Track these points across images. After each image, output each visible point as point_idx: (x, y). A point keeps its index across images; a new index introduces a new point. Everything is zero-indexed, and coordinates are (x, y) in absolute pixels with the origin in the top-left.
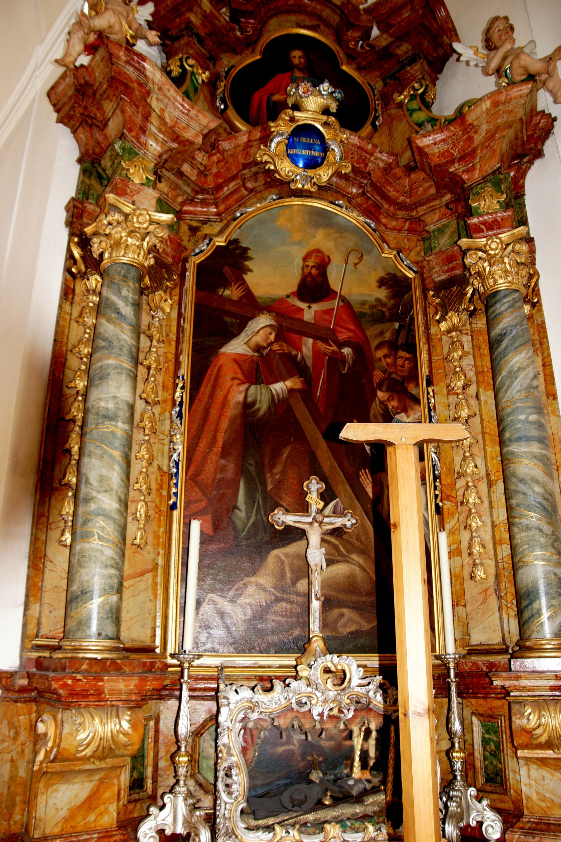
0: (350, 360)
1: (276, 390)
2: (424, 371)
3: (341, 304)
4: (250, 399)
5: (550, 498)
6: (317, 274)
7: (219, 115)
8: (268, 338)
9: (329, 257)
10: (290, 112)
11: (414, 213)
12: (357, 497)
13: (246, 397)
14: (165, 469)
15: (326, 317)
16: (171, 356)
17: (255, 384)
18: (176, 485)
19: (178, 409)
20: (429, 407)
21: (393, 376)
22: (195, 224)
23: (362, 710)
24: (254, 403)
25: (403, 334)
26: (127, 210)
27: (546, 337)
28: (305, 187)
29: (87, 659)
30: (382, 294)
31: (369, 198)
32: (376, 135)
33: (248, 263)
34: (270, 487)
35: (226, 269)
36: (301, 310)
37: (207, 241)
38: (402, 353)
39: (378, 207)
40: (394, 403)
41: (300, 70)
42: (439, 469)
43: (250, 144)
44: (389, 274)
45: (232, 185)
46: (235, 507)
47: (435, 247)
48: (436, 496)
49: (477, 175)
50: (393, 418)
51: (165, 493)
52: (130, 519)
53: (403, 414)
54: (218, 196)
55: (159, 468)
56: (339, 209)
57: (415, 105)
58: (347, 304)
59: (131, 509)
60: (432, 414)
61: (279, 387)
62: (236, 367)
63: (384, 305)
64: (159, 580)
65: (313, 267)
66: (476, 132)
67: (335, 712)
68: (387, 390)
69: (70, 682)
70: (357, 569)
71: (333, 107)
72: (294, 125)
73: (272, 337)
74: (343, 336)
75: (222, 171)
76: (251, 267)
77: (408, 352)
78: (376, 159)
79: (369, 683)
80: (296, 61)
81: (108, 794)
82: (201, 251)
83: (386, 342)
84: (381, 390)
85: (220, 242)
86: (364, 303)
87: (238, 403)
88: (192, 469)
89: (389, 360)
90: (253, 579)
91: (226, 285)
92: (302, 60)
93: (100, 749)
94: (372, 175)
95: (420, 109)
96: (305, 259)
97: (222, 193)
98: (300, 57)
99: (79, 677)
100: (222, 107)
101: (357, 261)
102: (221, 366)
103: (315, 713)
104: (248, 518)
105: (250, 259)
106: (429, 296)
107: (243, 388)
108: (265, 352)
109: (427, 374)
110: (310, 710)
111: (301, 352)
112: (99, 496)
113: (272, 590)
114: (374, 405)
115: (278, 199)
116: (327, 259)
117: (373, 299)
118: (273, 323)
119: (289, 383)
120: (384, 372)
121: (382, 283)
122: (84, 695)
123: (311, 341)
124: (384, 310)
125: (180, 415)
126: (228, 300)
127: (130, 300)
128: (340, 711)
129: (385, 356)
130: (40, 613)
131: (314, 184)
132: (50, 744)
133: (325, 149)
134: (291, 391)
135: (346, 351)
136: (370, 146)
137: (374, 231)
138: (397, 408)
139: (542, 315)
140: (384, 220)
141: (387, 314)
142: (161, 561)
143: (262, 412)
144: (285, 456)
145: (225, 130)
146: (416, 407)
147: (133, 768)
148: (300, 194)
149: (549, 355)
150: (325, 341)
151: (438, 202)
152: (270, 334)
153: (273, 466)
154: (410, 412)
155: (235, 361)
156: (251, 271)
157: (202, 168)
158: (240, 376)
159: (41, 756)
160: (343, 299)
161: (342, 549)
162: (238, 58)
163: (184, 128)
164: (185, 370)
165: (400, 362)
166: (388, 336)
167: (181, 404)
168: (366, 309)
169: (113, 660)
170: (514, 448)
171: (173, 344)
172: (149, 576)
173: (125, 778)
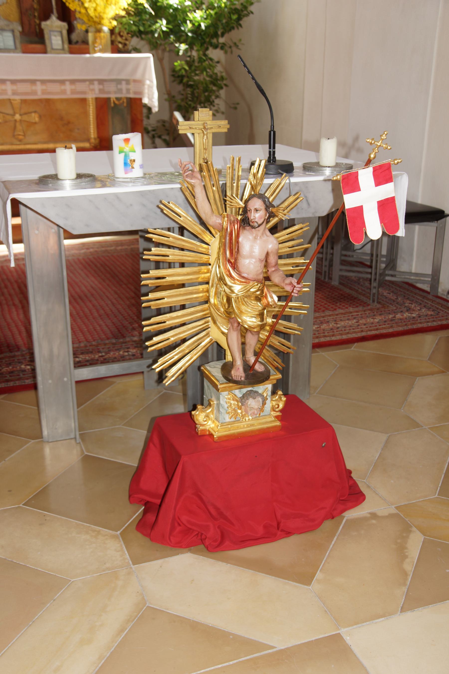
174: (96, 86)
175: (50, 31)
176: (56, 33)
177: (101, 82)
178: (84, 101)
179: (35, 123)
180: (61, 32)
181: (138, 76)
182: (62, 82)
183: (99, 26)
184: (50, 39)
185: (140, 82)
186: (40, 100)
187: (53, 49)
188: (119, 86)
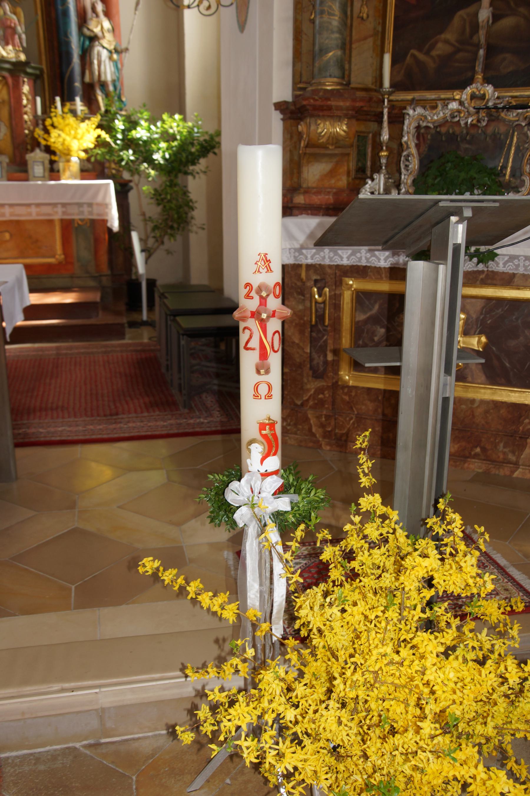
23: (493, 121)
29: (322, 89)
64: (379, 43)
67: (474, 122)
69: (312, 101)
90: (443, 36)
93: (331, 139)
99: (316, 98)
103: (462, 123)
110: (459, 120)
113: (457, 44)
122: (321, 108)
128: (479, 121)
132: (305, 136)
142: (380, 29)
147: (358, 161)
159: (302, 144)
169: (338, 90)
173: (352, 165)
174: (60, 209)
175: (34, 162)
176: (39, 164)
177: (64, 205)
178: (51, 222)
179: (6, 241)
180: (43, 163)
181: (99, 199)
182: (29, 205)
183: (68, 157)
184: (33, 169)
185: (106, 206)
186: (11, 222)
187: (34, 177)
188: (81, 209)
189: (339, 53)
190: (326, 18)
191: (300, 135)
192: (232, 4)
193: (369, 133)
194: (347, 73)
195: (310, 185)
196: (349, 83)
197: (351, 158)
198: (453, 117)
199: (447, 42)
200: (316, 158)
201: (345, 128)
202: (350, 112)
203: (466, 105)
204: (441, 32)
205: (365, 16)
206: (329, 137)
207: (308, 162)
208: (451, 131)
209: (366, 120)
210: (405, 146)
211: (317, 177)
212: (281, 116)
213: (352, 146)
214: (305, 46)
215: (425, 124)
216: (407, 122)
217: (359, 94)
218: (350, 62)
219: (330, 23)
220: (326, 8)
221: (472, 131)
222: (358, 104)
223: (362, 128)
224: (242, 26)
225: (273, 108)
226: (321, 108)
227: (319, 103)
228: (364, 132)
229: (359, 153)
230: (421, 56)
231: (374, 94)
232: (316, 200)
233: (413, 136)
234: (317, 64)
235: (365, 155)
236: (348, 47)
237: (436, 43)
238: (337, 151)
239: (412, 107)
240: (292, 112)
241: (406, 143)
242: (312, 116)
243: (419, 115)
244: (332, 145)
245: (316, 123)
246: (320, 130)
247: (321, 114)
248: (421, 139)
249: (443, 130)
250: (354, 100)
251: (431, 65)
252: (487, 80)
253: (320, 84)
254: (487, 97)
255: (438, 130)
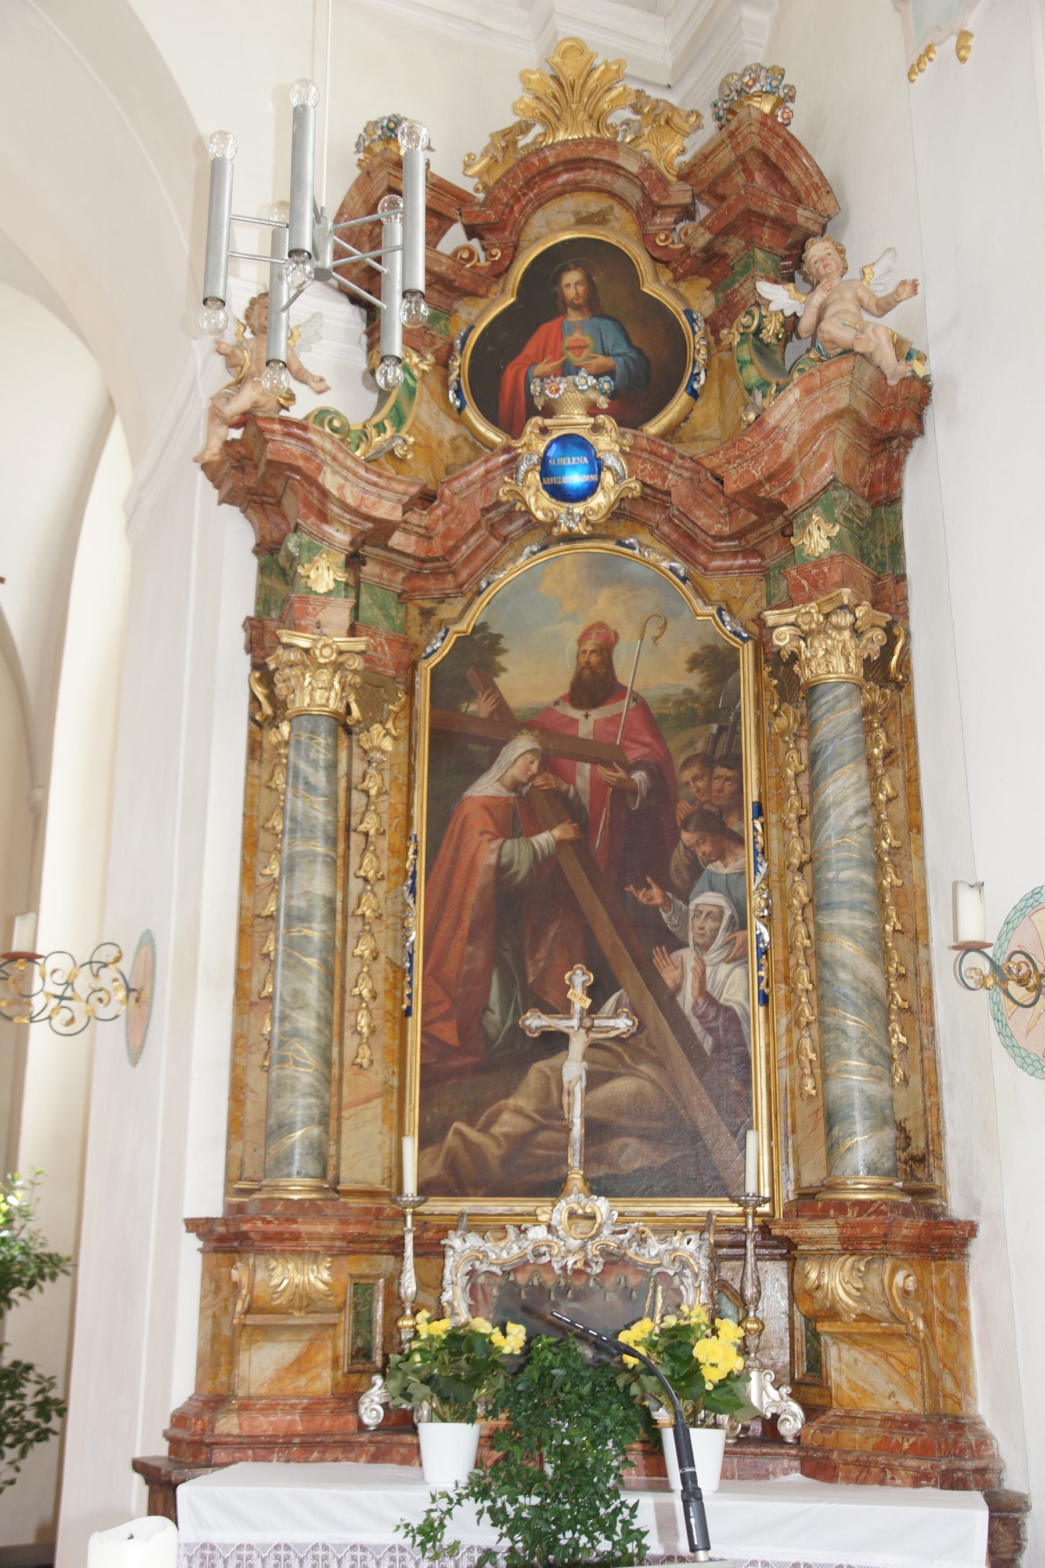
0: (643, 789)
1: (539, 844)
2: (752, 794)
3: (633, 705)
4: (504, 860)
5: (862, 987)
6: (599, 663)
7: (456, 415)
8: (528, 769)
9: (616, 634)
10: (538, 420)
11: (743, 543)
12: (649, 988)
13: (499, 857)
14: (399, 963)
15: (611, 729)
16: (401, 808)
17: (512, 837)
18: (410, 983)
19: (410, 882)
20: (755, 849)
21: (707, 806)
22: (427, 604)
23: (614, 1263)
24: (510, 864)
25: (724, 739)
26: (305, 643)
27: (914, 736)
28: (576, 529)
29: (281, 1199)
30: (694, 681)
31: (677, 526)
32: (700, 402)
33: (501, 659)
34: (531, 980)
35: (471, 674)
36: (574, 722)
37: (442, 634)
38: (721, 771)
39: (692, 540)
40: (706, 848)
41: (577, 308)
42: (767, 938)
43: (490, 476)
44: (707, 647)
45: (473, 540)
46: (487, 1008)
47: (775, 595)
48: (760, 979)
49: (802, 497)
50: (703, 870)
51: (398, 994)
52: (347, 1033)
53: (718, 863)
54: (453, 561)
55: (391, 962)
56: (630, 551)
57: (746, 353)
58: (641, 705)
59: (349, 1020)
60: (759, 859)
61: (544, 839)
62: (486, 816)
63: (696, 699)
64: (394, 1106)
65: (593, 652)
66: (785, 438)
67: (579, 1265)
68: (698, 828)
69: (259, 1224)
70: (647, 1084)
71: (603, 402)
72: (548, 440)
73: (534, 768)
74: (634, 754)
75: (453, 526)
76: (504, 665)
77: (728, 767)
78: (677, 466)
79: (625, 1231)
80: (570, 293)
81: (320, 1358)
82: (434, 651)
83: (696, 756)
84: (686, 829)
85: (465, 626)
86: (665, 700)
87: (489, 867)
88: (431, 961)
89: (700, 784)
90: (511, 1102)
91: (471, 696)
92: (581, 289)
93: (297, 1297)
94: (673, 494)
95: (751, 362)
96: (581, 641)
97: (458, 556)
98: (577, 283)
99: (269, 1217)
100: (458, 403)
101: (657, 633)
102: (466, 817)
103: (556, 1267)
104: (503, 1023)
105: (504, 651)
106: (765, 674)
107: (495, 845)
108: (525, 790)
109: (756, 799)
111: (574, 784)
112: (294, 1014)
114: (675, 853)
115: (539, 551)
116: (613, 636)
117: (680, 691)
118: (536, 746)
119: (557, 833)
120: (692, 803)
121: (694, 663)
123: (588, 767)
124: (697, 706)
125: (413, 890)
126: (474, 718)
127: (322, 764)
128: (587, 1264)
129: (695, 779)
130: (243, 1151)
131: (588, 522)
132: (244, 1292)
133: (597, 466)
134: (560, 843)
135: (639, 776)
136: (665, 451)
137: (684, 580)
138: (710, 854)
139: (912, 702)
140: (703, 558)
141: (701, 712)
142: (395, 1082)
143: (520, 877)
144: (551, 935)
145: (466, 439)
146: (738, 851)
147: (356, 1334)
148: (571, 538)
149: (916, 765)
150: (608, 765)
151: (769, 527)
152: (532, 763)
153: (535, 950)
154: (730, 859)
155: (485, 807)
156: (504, 670)
157: (422, 531)
158: (491, 828)
160: (636, 697)
161: (626, 1058)
162: (482, 303)
163: (374, 504)
164: (420, 827)
165: (717, 784)
166: (700, 746)
167: (414, 876)
168: (669, 709)
170: (825, 920)
171: (405, 789)
172: (377, 1104)
173: (344, 1344)
189: (316, 1131)
190: (290, 1070)
191: (236, 1286)
192: (117, 1017)
193: (378, 1277)
194: (332, 1162)
195: (253, 1391)
196: (337, 1181)
197: (341, 1329)
198: (538, 1255)
199: (518, 1111)
200: (266, 1332)
201: (325, 1275)
202: (338, 1243)
203: (561, 1233)
204: (508, 1095)
205: (365, 1063)
206: (294, 1294)
207: (251, 1343)
208: (536, 1283)
209: (371, 1253)
210: (448, 1310)
211: (269, 1373)
212: (200, 1244)
213: (340, 1309)
214: (253, 1111)
215: (484, 1267)
216: (449, 1262)
217: (354, 1203)
218: (338, 1142)
219: (298, 1079)
220: (290, 1054)
221: (579, 1283)
222: (353, 1230)
223: (361, 1266)
224: (135, 1054)
225: (184, 1228)
226: (278, 1237)
227: (272, 1228)
228: (367, 1277)
229: (357, 1319)
230: (472, 1134)
231: (385, 1201)
232: (265, 1424)
233: (464, 1291)
234: (272, 1151)
235: (370, 1322)
236: (334, 1115)
237: (499, 1112)
238: (311, 1319)
239: (459, 1233)
240: (221, 1239)
241: (450, 1303)
242: (260, 1251)
243: (473, 1249)
244: (300, 1309)
245: (267, 1267)
246: (275, 1281)
247: (278, 1248)
248: (480, 1296)
249: (521, 1278)
250: (344, 1222)
251: (494, 1151)
252: (597, 1187)
253: (277, 1188)
254: (599, 1220)
255: (511, 1278)
